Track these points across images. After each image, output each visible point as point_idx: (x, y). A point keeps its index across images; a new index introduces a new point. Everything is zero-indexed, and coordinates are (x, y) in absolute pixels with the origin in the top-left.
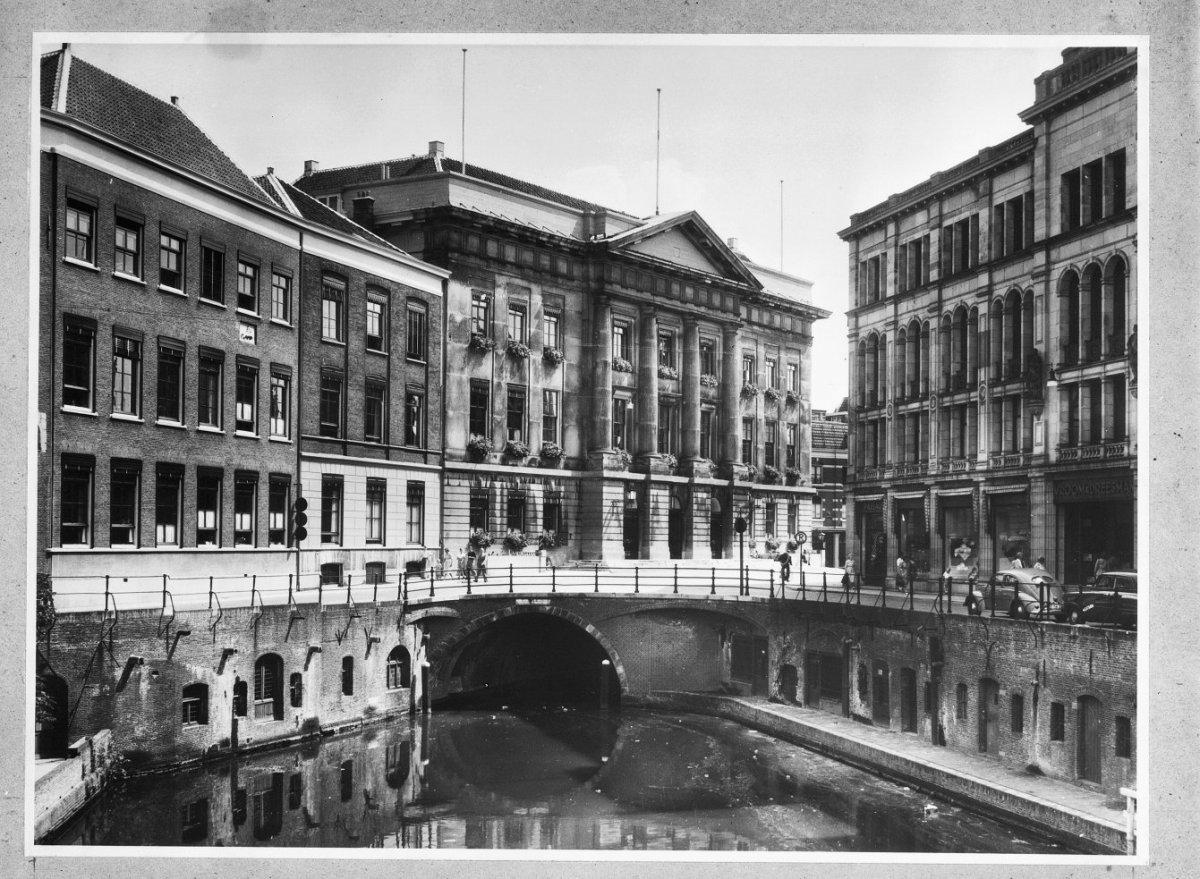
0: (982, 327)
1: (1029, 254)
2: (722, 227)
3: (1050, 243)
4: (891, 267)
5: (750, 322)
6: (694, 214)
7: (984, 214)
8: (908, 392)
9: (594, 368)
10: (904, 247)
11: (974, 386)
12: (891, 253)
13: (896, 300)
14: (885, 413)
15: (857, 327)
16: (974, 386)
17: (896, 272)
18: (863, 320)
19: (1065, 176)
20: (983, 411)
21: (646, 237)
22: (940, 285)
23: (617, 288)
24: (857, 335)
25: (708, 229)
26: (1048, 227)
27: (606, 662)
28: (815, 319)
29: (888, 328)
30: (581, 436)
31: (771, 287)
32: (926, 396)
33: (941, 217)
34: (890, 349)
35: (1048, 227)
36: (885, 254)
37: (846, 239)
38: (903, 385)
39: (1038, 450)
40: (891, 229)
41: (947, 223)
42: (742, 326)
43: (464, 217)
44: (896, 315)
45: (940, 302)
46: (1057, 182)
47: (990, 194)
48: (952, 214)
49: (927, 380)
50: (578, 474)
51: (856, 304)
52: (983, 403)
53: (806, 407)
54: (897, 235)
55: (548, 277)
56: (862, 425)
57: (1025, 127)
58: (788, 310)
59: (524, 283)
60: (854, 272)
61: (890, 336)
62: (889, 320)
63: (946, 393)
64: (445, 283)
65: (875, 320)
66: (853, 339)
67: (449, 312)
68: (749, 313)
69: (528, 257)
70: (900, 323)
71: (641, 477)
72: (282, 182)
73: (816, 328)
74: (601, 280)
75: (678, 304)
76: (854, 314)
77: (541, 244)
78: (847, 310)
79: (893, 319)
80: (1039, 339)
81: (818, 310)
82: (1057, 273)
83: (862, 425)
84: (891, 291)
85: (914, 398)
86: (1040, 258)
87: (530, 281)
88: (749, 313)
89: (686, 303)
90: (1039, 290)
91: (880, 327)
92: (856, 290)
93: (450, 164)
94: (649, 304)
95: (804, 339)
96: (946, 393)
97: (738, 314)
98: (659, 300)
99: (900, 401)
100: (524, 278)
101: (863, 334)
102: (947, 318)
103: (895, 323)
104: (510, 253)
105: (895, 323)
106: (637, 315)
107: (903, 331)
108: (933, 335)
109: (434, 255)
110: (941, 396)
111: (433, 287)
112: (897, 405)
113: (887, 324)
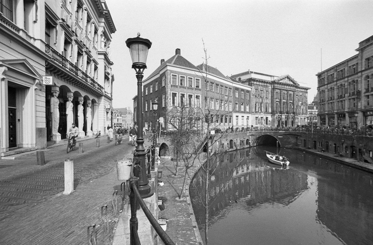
0: (346, 87)
1: (357, 73)
2: (292, 77)
3: (362, 71)
4: (326, 79)
5: (297, 91)
6: (288, 75)
7: (346, 68)
8: (330, 99)
10: (329, 76)
11: (344, 97)
12: (326, 77)
13: (327, 84)
14: (325, 103)
16: (344, 97)
18: (320, 88)
19: (366, 59)
20: (346, 101)
22: (336, 81)
23: (276, 87)
25: (291, 77)
26: (362, 68)
27: (277, 141)
30: (272, 109)
32: (334, 99)
33: (337, 70)
34: (326, 93)
35: (362, 68)
39: (359, 107)
40: (326, 73)
41: (338, 71)
44: (327, 87)
45: (337, 84)
46: (364, 60)
47: (348, 65)
48: (339, 69)
49: (334, 97)
50: (271, 115)
52: (346, 100)
54: (327, 74)
56: (321, 105)
57: (358, 53)
61: (326, 90)
63: (338, 98)
64: (251, 88)
65: (322, 88)
69: (263, 84)
71: (288, 115)
74: (274, 86)
76: (319, 88)
77: (265, 82)
80: (359, 88)
82: (364, 76)
83: (321, 105)
84: (326, 83)
85: (331, 100)
86: (360, 74)
90: (359, 79)
91: (324, 89)
93: (252, 72)
94: (281, 89)
95: (307, 92)
96: (338, 98)
99: (329, 100)
100: (263, 87)
101: (320, 90)
102: (338, 86)
103: (327, 88)
104: (261, 84)
105: (327, 88)
108: (335, 90)
109: (250, 85)
110: (337, 99)
111: (250, 89)
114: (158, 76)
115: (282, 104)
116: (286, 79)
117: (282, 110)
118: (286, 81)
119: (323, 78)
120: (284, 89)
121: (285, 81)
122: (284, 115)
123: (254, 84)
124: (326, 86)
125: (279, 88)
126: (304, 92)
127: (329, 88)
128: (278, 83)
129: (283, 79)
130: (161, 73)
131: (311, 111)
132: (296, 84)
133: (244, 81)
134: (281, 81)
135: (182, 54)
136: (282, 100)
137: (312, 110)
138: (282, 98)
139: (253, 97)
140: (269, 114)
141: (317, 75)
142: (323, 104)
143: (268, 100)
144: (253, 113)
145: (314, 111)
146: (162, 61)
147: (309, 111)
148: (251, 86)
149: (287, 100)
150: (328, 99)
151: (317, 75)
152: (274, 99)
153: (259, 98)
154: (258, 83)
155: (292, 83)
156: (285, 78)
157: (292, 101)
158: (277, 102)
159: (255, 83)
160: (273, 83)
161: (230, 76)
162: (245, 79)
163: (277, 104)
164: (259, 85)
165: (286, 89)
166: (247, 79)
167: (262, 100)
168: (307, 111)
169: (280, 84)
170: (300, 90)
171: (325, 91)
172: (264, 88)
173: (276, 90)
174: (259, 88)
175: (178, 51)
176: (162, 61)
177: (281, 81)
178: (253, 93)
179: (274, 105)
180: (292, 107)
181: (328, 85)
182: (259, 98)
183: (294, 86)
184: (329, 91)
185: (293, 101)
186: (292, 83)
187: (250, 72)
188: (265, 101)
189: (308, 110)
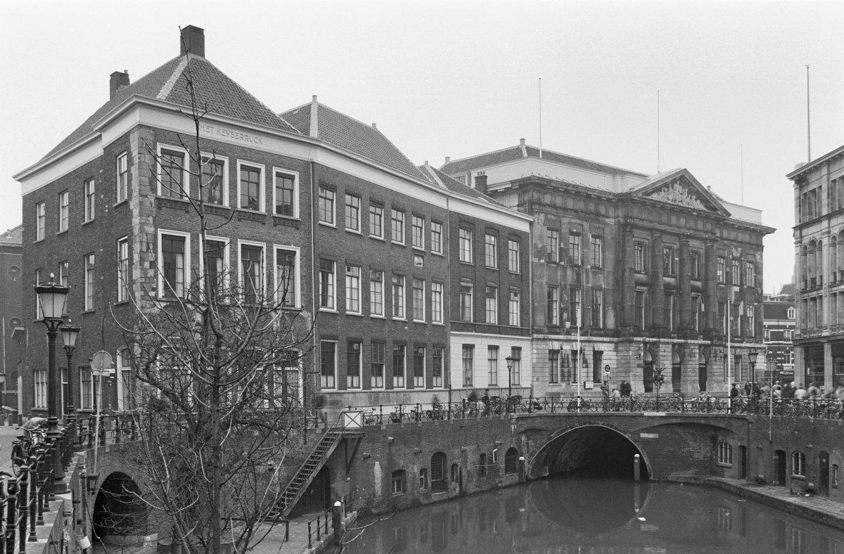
2: (704, 178)
4: (824, 195)
5: (722, 238)
9: (623, 273)
10: (834, 181)
12: (825, 186)
13: (829, 217)
14: (822, 292)
15: (801, 237)
17: (828, 198)
18: (805, 232)
21: (657, 189)
23: (637, 221)
24: (801, 242)
28: (764, 235)
29: (823, 236)
30: (616, 316)
31: (736, 215)
34: (825, 249)
36: (820, 187)
37: (792, 179)
38: (835, 273)
40: (824, 171)
42: (717, 241)
43: (543, 183)
44: (829, 227)
50: (615, 340)
51: (800, 221)
53: (760, 292)
54: (828, 174)
55: (593, 216)
56: (806, 301)
58: (747, 229)
59: (578, 222)
60: (798, 200)
61: (825, 241)
62: (823, 231)
64: (531, 224)
65: (812, 232)
66: (799, 245)
67: (534, 242)
68: (721, 233)
69: (580, 205)
70: (832, 233)
72: (435, 170)
73: (766, 240)
75: (676, 229)
76: (800, 228)
77: (589, 196)
78: (794, 226)
79: (827, 230)
81: (768, 228)
83: (806, 301)
84: (825, 212)
87: (582, 220)
88: (721, 233)
89: (680, 228)
91: (818, 237)
92: (800, 212)
93: (533, 152)
94: (657, 230)
95: (760, 247)
97: (714, 234)
98: (663, 227)
99: (834, 284)
100: (579, 218)
101: (806, 241)
104: (570, 204)
105: (829, 232)
106: (650, 238)
107: (834, 238)
111: (525, 227)
112: (830, 287)
113: (823, 234)
114: (95, 152)
115: (660, 295)
116: (677, 186)
117: (660, 320)
118: (677, 196)
119: (814, 191)
120: (669, 229)
121: (671, 197)
122: (666, 340)
123: (541, 204)
124: (825, 224)
125: (646, 224)
126: (748, 246)
127: (836, 231)
128: (643, 203)
129: (666, 186)
130: (109, 137)
131: (778, 327)
132: (715, 209)
133: (501, 189)
134: (655, 197)
135: (214, 54)
136: (661, 275)
137: (781, 323)
138: (661, 270)
139: (536, 260)
140: (607, 336)
141: (791, 176)
142: (814, 299)
143: (601, 276)
144: (539, 332)
145: (788, 324)
146: (119, 80)
147: (770, 327)
148: (531, 212)
149: (681, 276)
150: (832, 279)
151: (791, 176)
152: (627, 274)
153: (564, 268)
154: (559, 201)
155: (699, 205)
156: (674, 182)
157: (699, 284)
158: (639, 283)
159: (547, 199)
160: (624, 200)
161: (439, 164)
162: (506, 183)
163: (641, 293)
164: (565, 209)
165: (676, 230)
166: (512, 182)
167: (578, 275)
168: (759, 325)
169: (654, 204)
170: (733, 235)
171: (821, 242)
172: (586, 225)
173: (637, 233)
174: (565, 220)
175: (192, 38)
176: (119, 80)
177: (655, 197)
178: (540, 246)
179: (628, 296)
180: (703, 310)
181: (834, 221)
182: (564, 268)
183: (707, 218)
184: (834, 245)
185: (706, 282)
186: (699, 205)
187: (528, 149)
188: (587, 282)
189: (766, 323)
